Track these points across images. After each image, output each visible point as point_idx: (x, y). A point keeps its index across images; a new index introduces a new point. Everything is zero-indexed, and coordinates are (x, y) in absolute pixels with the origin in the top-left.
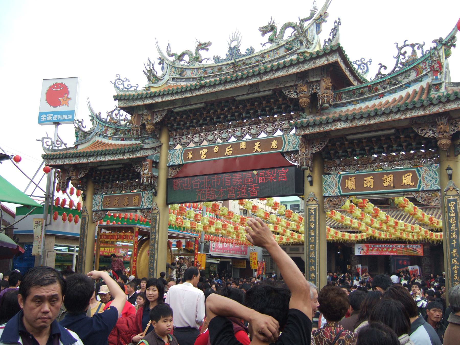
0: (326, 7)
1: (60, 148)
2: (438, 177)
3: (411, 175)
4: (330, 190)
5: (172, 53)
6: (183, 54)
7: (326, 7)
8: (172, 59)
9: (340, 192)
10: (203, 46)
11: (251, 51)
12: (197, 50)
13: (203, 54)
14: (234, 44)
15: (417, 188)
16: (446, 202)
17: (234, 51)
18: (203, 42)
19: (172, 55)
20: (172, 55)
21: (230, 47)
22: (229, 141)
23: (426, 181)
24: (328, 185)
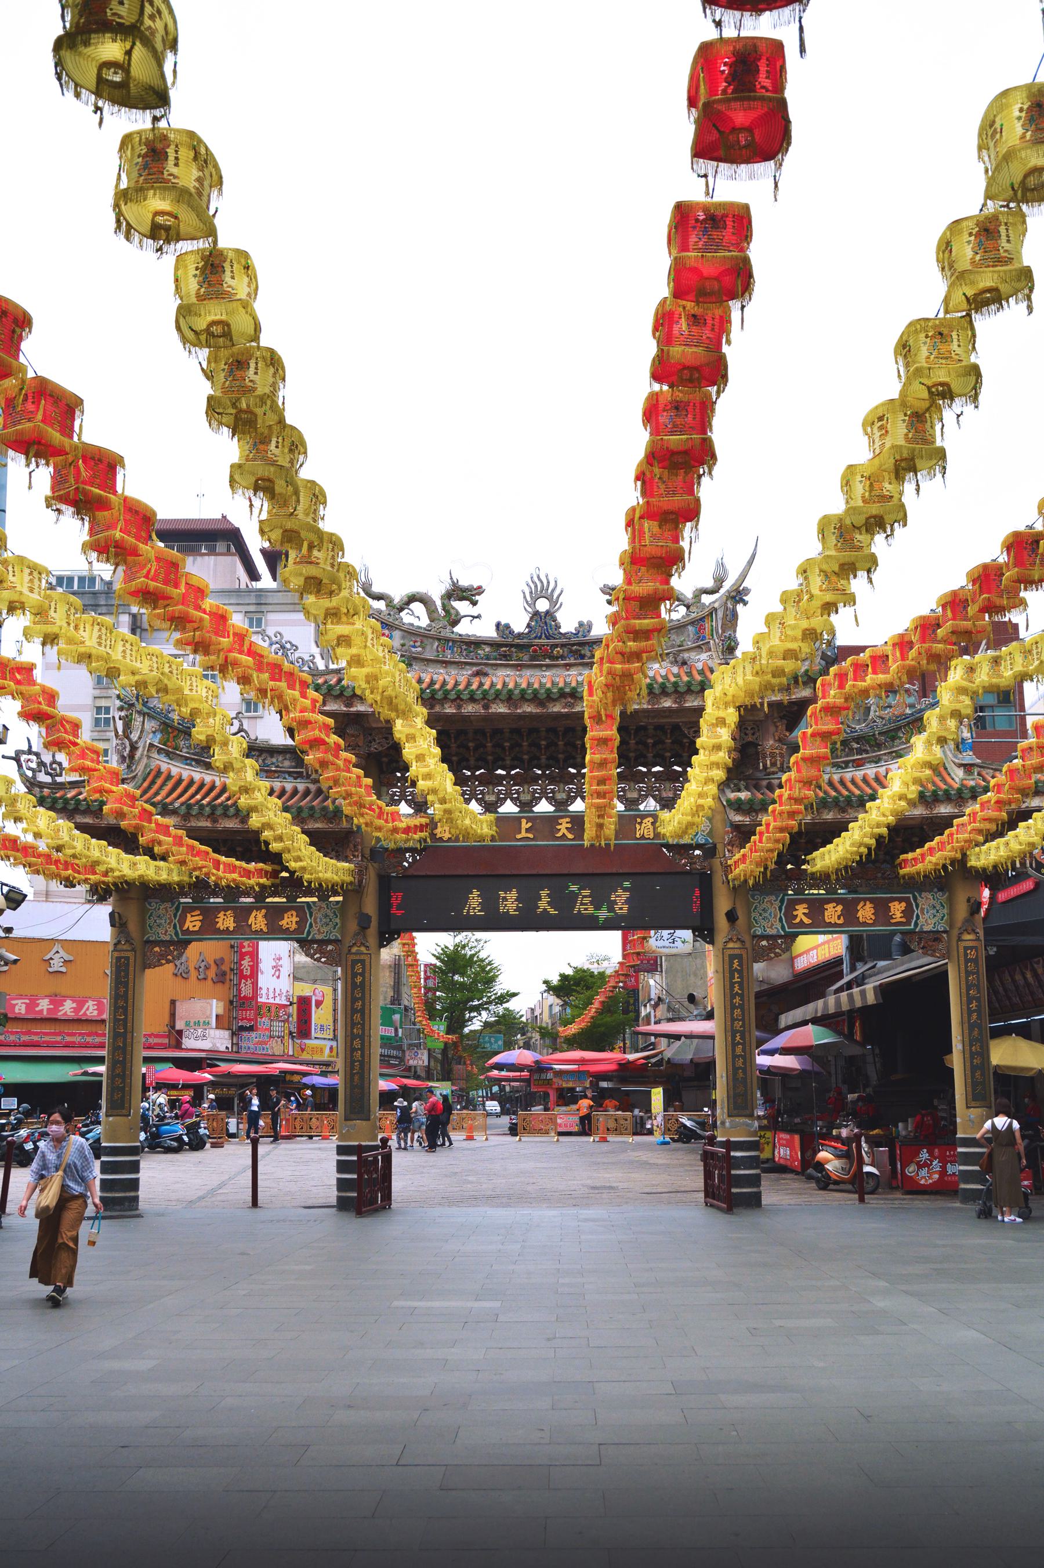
0: (744, 576)
1: (59, 779)
2: (945, 911)
3: (903, 904)
4: (763, 923)
5: (376, 589)
6: (412, 599)
7: (744, 576)
8: (381, 605)
9: (783, 928)
10: (468, 594)
11: (585, 627)
12: (449, 596)
13: (462, 607)
14: (543, 605)
15: (912, 927)
16: (961, 951)
17: (543, 621)
18: (464, 583)
19: (379, 597)
20: (379, 597)
21: (536, 614)
22: (535, 809)
23: (926, 916)
24: (761, 915)
